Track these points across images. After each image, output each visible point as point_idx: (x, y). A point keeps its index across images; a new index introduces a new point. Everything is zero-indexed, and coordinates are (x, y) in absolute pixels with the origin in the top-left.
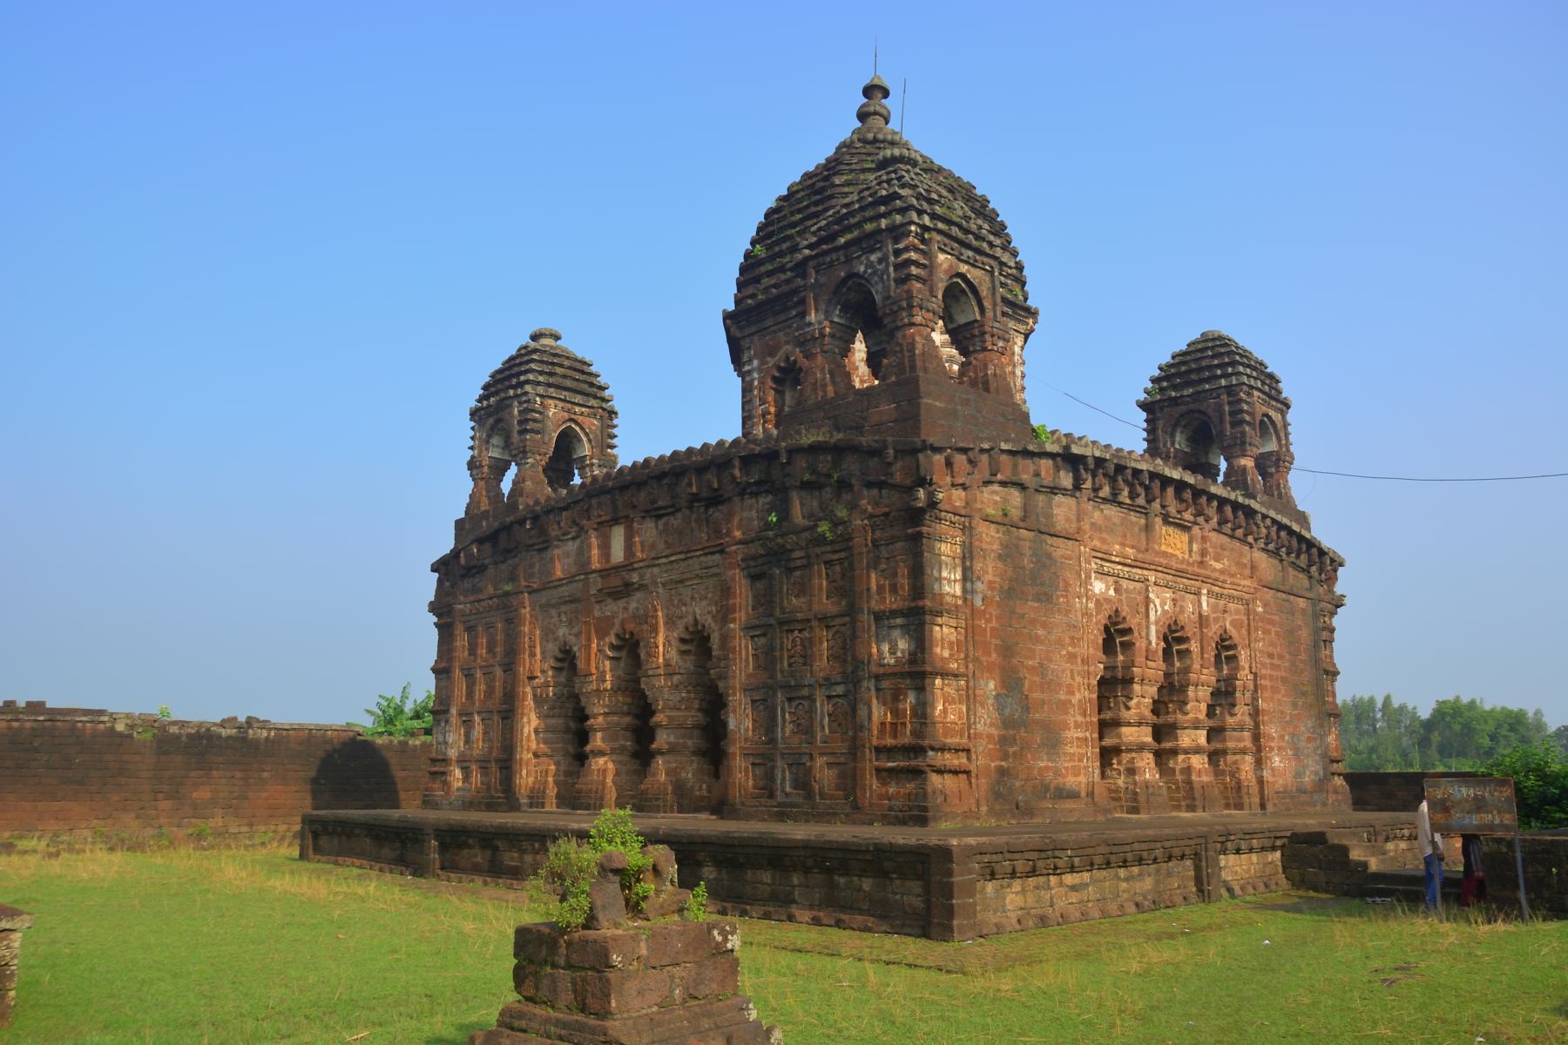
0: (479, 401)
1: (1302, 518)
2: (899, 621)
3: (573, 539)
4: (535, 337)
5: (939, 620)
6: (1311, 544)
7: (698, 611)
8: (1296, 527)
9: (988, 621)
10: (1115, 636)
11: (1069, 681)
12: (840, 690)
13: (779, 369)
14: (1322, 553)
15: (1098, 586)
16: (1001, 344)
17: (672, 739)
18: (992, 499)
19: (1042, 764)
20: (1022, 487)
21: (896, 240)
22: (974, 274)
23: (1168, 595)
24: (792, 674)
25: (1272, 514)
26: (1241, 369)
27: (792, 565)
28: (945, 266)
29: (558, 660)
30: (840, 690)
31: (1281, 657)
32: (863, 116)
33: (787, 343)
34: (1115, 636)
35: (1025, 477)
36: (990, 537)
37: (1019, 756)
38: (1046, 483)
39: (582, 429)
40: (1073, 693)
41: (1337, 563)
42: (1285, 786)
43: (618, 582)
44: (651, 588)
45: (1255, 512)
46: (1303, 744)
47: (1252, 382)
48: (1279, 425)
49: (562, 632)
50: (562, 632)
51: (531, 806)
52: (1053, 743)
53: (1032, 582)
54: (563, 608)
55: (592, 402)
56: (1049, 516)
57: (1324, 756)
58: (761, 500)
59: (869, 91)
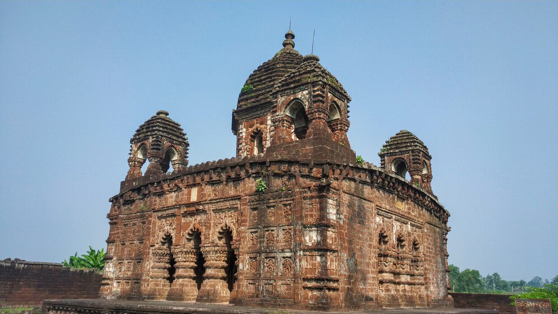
0: (135, 135)
1: (436, 197)
2: (314, 229)
3: (175, 191)
4: (158, 114)
5: (329, 229)
6: (441, 208)
7: (227, 222)
8: (437, 201)
9: (345, 230)
10: (382, 238)
11: (369, 255)
13: (254, 132)
14: (444, 211)
15: (378, 219)
16: (346, 128)
17: (213, 272)
18: (345, 184)
19: (361, 287)
20: (355, 180)
21: (314, 87)
22: (339, 102)
23: (398, 224)
24: (268, 247)
25: (430, 196)
26: (416, 144)
28: (330, 98)
29: (163, 238)
31: (432, 249)
32: (285, 45)
33: (257, 123)
34: (382, 238)
35: (356, 177)
36: (346, 198)
37: (354, 283)
38: (362, 179)
39: (176, 149)
40: (370, 259)
41: (448, 215)
42: (434, 298)
43: (194, 210)
45: (426, 195)
46: (439, 282)
47: (420, 149)
48: (428, 165)
49: (166, 228)
51: (148, 298)
52: (364, 279)
53: (358, 216)
55: (180, 140)
56: (363, 192)
57: (446, 286)
59: (287, 36)
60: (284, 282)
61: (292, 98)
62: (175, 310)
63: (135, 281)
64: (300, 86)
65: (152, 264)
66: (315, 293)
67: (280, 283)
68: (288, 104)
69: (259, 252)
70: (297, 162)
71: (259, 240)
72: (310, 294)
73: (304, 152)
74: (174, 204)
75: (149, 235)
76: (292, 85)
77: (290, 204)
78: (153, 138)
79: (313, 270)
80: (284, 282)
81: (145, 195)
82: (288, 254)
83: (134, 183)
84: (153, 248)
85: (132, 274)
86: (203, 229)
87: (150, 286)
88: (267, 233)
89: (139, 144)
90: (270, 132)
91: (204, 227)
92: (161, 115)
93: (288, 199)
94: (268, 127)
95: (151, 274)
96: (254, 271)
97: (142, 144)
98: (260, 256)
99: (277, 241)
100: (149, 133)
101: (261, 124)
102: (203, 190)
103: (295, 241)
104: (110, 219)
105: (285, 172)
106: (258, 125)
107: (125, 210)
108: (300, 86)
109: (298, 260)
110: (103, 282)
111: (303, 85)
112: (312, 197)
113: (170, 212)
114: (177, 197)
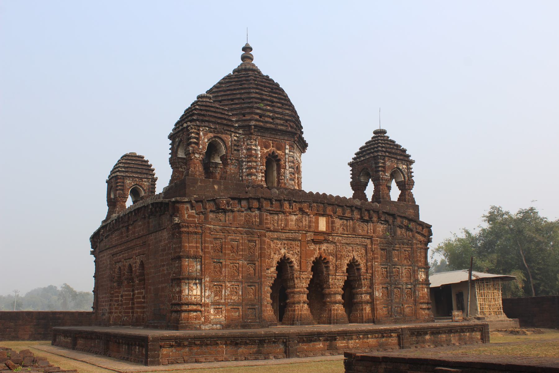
3: (294, 215)
12: (409, 286)
30: (409, 286)
33: (273, 147)
43: (320, 238)
44: (338, 244)
49: (283, 251)
50: (283, 251)
54: (286, 242)
63: (248, 307)
66: (427, 311)
67: (406, 306)
69: (390, 284)
71: (389, 275)
74: (295, 228)
75: (264, 257)
76: (398, 157)
79: (423, 298)
81: (250, 208)
83: (216, 187)
85: (243, 300)
88: (394, 270)
89: (211, 135)
91: (331, 257)
94: (287, 156)
96: (385, 298)
97: (215, 137)
98: (391, 286)
99: (402, 277)
101: (279, 149)
105: (405, 226)
106: (274, 149)
107: (212, 219)
110: (185, 308)
111: (405, 160)
112: (421, 248)
113: (290, 235)
114: (299, 221)
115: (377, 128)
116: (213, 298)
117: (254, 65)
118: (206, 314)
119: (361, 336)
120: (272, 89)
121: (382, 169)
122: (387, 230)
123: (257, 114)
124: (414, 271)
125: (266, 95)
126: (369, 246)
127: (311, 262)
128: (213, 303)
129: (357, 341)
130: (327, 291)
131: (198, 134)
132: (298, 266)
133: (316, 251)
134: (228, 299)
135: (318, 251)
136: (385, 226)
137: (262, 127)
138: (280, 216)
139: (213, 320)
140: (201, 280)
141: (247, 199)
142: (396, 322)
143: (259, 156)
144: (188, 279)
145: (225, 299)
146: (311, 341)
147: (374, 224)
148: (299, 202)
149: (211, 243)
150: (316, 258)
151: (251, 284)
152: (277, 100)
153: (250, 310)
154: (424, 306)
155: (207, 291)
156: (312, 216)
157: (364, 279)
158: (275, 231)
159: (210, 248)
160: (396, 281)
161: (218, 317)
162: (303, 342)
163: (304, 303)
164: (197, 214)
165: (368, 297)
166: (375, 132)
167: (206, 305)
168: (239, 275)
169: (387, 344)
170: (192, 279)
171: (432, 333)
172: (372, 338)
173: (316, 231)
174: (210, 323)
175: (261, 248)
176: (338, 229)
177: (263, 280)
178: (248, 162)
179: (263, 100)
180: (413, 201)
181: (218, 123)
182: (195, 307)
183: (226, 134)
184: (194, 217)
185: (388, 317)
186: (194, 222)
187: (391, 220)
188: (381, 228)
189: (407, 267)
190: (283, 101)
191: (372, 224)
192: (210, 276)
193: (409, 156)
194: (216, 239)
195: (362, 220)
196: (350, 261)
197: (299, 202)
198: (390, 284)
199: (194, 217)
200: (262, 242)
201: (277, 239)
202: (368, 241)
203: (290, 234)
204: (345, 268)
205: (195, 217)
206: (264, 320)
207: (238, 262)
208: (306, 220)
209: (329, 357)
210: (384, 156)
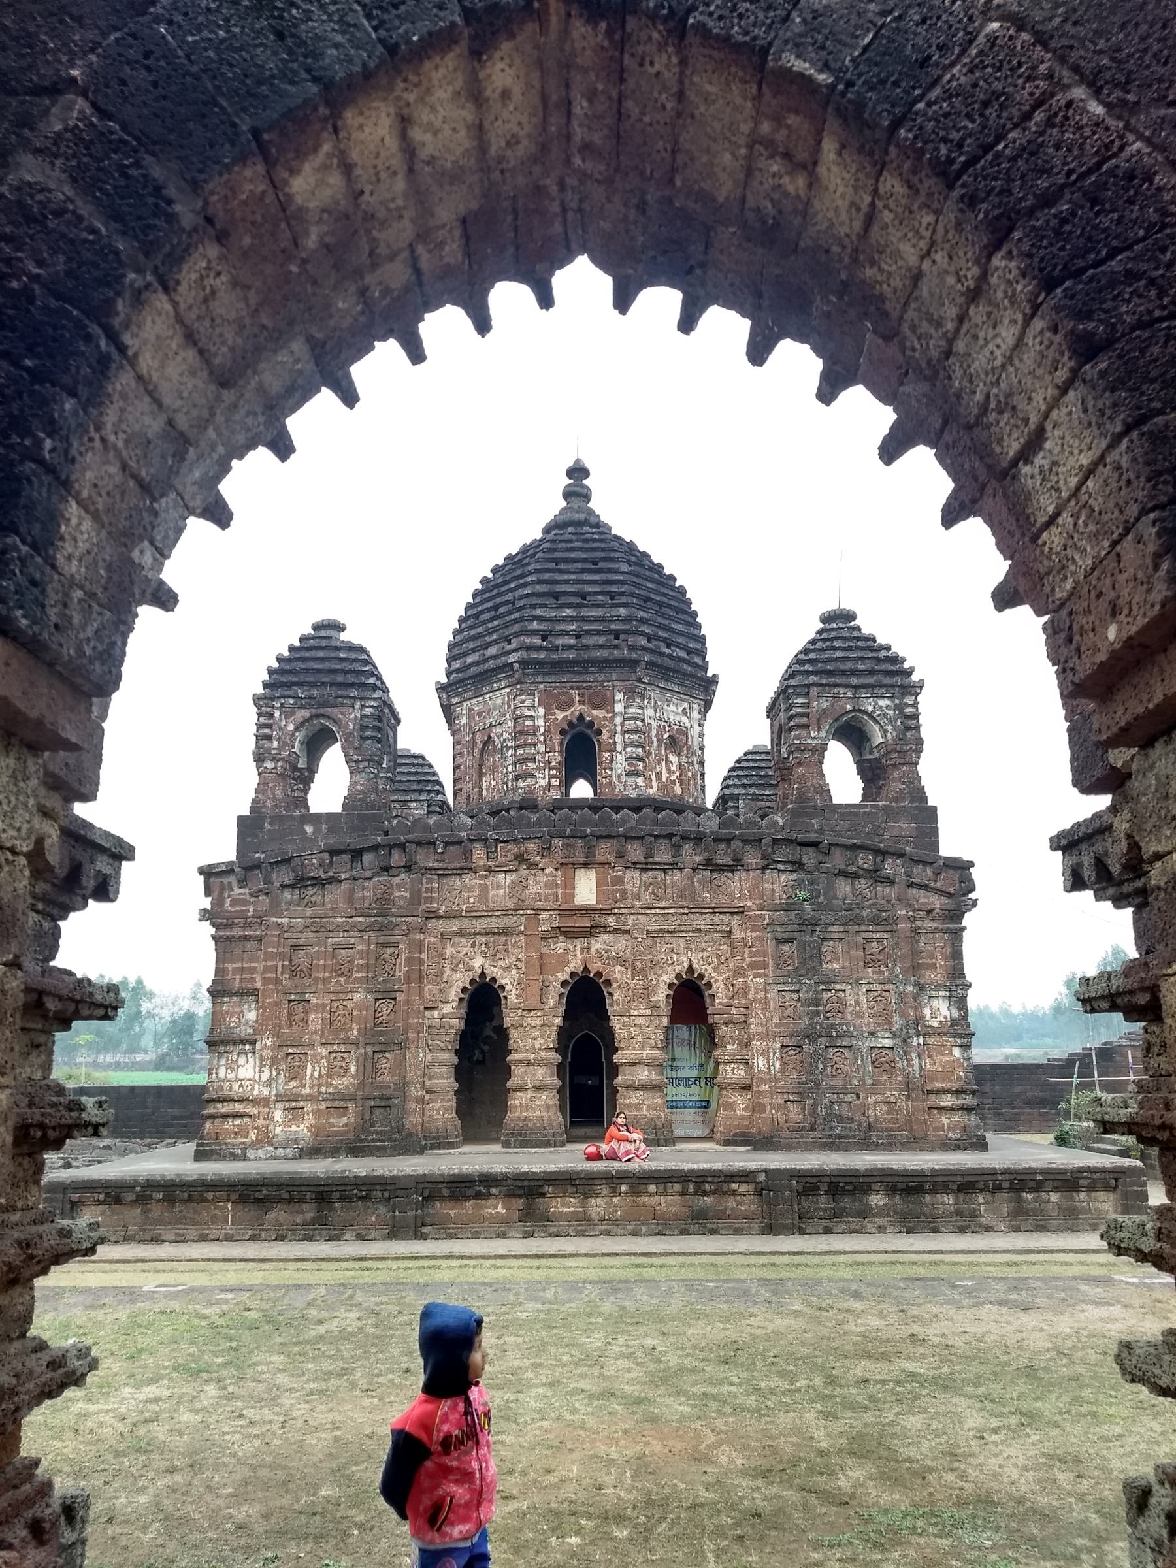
4: (316, 627)
27: (828, 936)
32: (568, 495)
43: (581, 925)
50: (478, 962)
58: (783, 878)
59: (570, 473)
60: (879, 1098)
61: (849, 707)
62: (693, 1171)
63: (372, 1103)
64: (873, 686)
65: (429, 1057)
67: (871, 1099)
68: (836, 720)
69: (812, 1036)
70: (901, 855)
72: (945, 1121)
73: (895, 832)
74: (509, 904)
76: (855, 681)
77: (879, 940)
78: (362, 706)
79: (946, 1075)
80: (879, 1098)
81: (386, 869)
82: (887, 1043)
83: (309, 829)
84: (436, 1014)
85: (362, 1084)
86: (619, 973)
87: (427, 1113)
88: (825, 996)
89: (306, 713)
90: (623, 733)
91: (618, 968)
92: (323, 633)
93: (879, 928)
94: (618, 720)
95: (427, 1083)
98: (814, 1041)
99: (859, 1015)
100: (354, 693)
102: (619, 880)
103: (903, 1015)
104: (217, 927)
106: (585, 708)
107: (290, 903)
108: (873, 686)
109: (914, 1055)
110: (211, 1110)
111: (882, 686)
112: (935, 931)
113: (493, 923)
115: (831, 605)
116: (282, 1084)
117: (591, 512)
118: (261, 1122)
119: (623, 1188)
120: (595, 563)
121: (804, 720)
122: (799, 884)
123: (533, 633)
124: (901, 996)
125: (567, 582)
126: (737, 934)
127: (557, 984)
128: (280, 1098)
129: (615, 1200)
130: (616, 1058)
131: (271, 716)
132: (518, 996)
133: (575, 957)
134: (319, 1086)
135: (579, 957)
136: (794, 876)
137: (541, 663)
138: (467, 879)
139: (276, 1137)
140: (254, 1043)
141: (376, 848)
142: (832, 1144)
143: (542, 730)
144: (222, 1043)
145: (312, 1087)
146: (467, 1198)
147: (752, 874)
148: (515, 840)
149: (283, 957)
150: (572, 974)
151: (383, 1048)
152: (597, 589)
153: (378, 1111)
154: (948, 1101)
155: (266, 1071)
156: (547, 871)
157: (726, 1024)
158: (448, 916)
159: (279, 970)
160: (833, 1026)
161: (294, 1128)
162: (442, 1198)
163: (538, 1088)
164: (251, 895)
165: (742, 1072)
166: (825, 619)
167: (264, 1102)
168: (351, 1029)
169: (721, 1215)
170: (235, 1043)
171: (892, 1190)
172: (665, 1193)
173: (564, 907)
174: (270, 1143)
175: (409, 961)
176: (637, 896)
177: (411, 1035)
178: (517, 748)
179: (556, 596)
180: (919, 795)
181: (313, 685)
182: (238, 1107)
183: (342, 704)
184: (244, 902)
185: (803, 1128)
186: (243, 915)
187: (810, 857)
188: (779, 884)
189: (874, 987)
190: (614, 588)
191: (744, 874)
192: (275, 1035)
193: (909, 673)
194: (295, 947)
195: (711, 865)
196: (678, 976)
197: (515, 840)
198: (811, 1036)
199: (244, 902)
200: (420, 946)
201: (461, 934)
202: (736, 921)
203: (493, 919)
204: (661, 995)
205: (250, 903)
206: (410, 1135)
207: (349, 996)
208: (537, 883)
209: (518, 1245)
210: (808, 686)
